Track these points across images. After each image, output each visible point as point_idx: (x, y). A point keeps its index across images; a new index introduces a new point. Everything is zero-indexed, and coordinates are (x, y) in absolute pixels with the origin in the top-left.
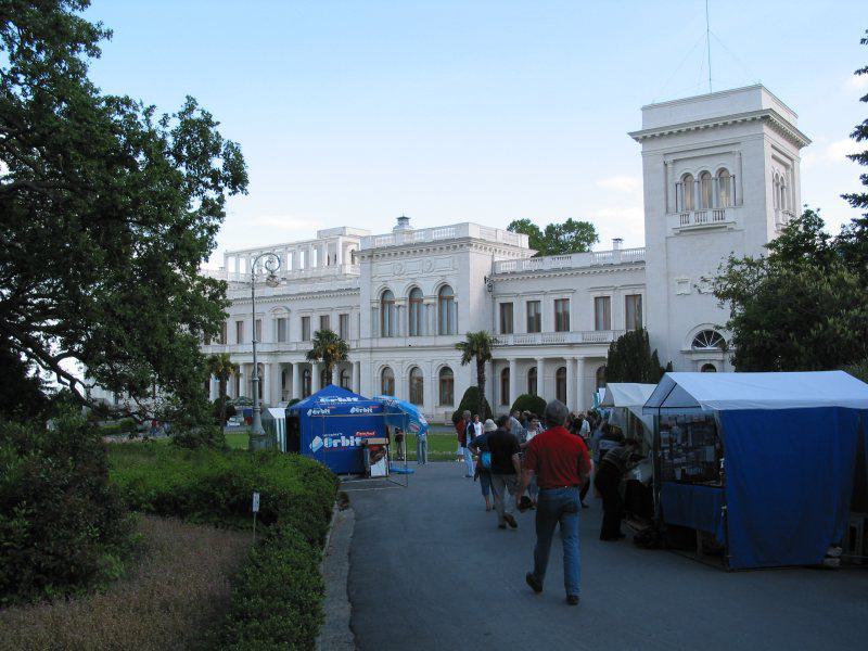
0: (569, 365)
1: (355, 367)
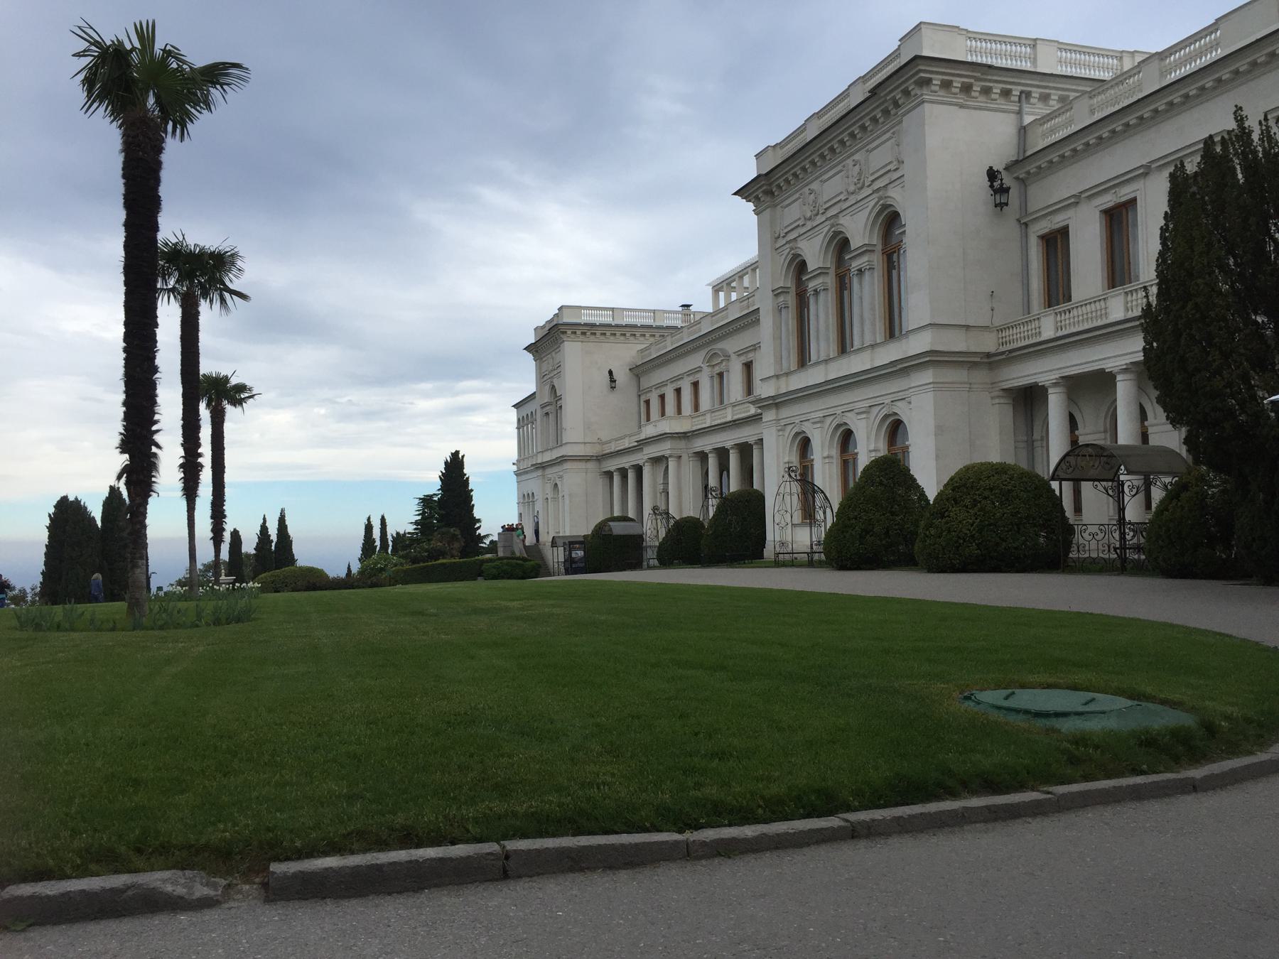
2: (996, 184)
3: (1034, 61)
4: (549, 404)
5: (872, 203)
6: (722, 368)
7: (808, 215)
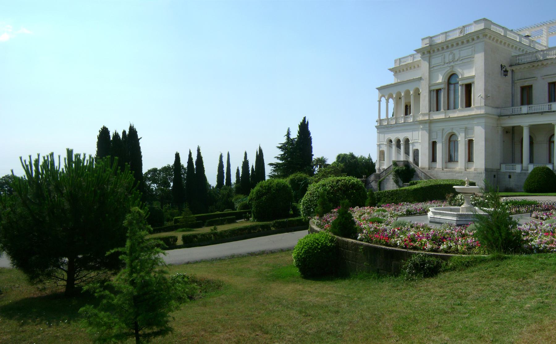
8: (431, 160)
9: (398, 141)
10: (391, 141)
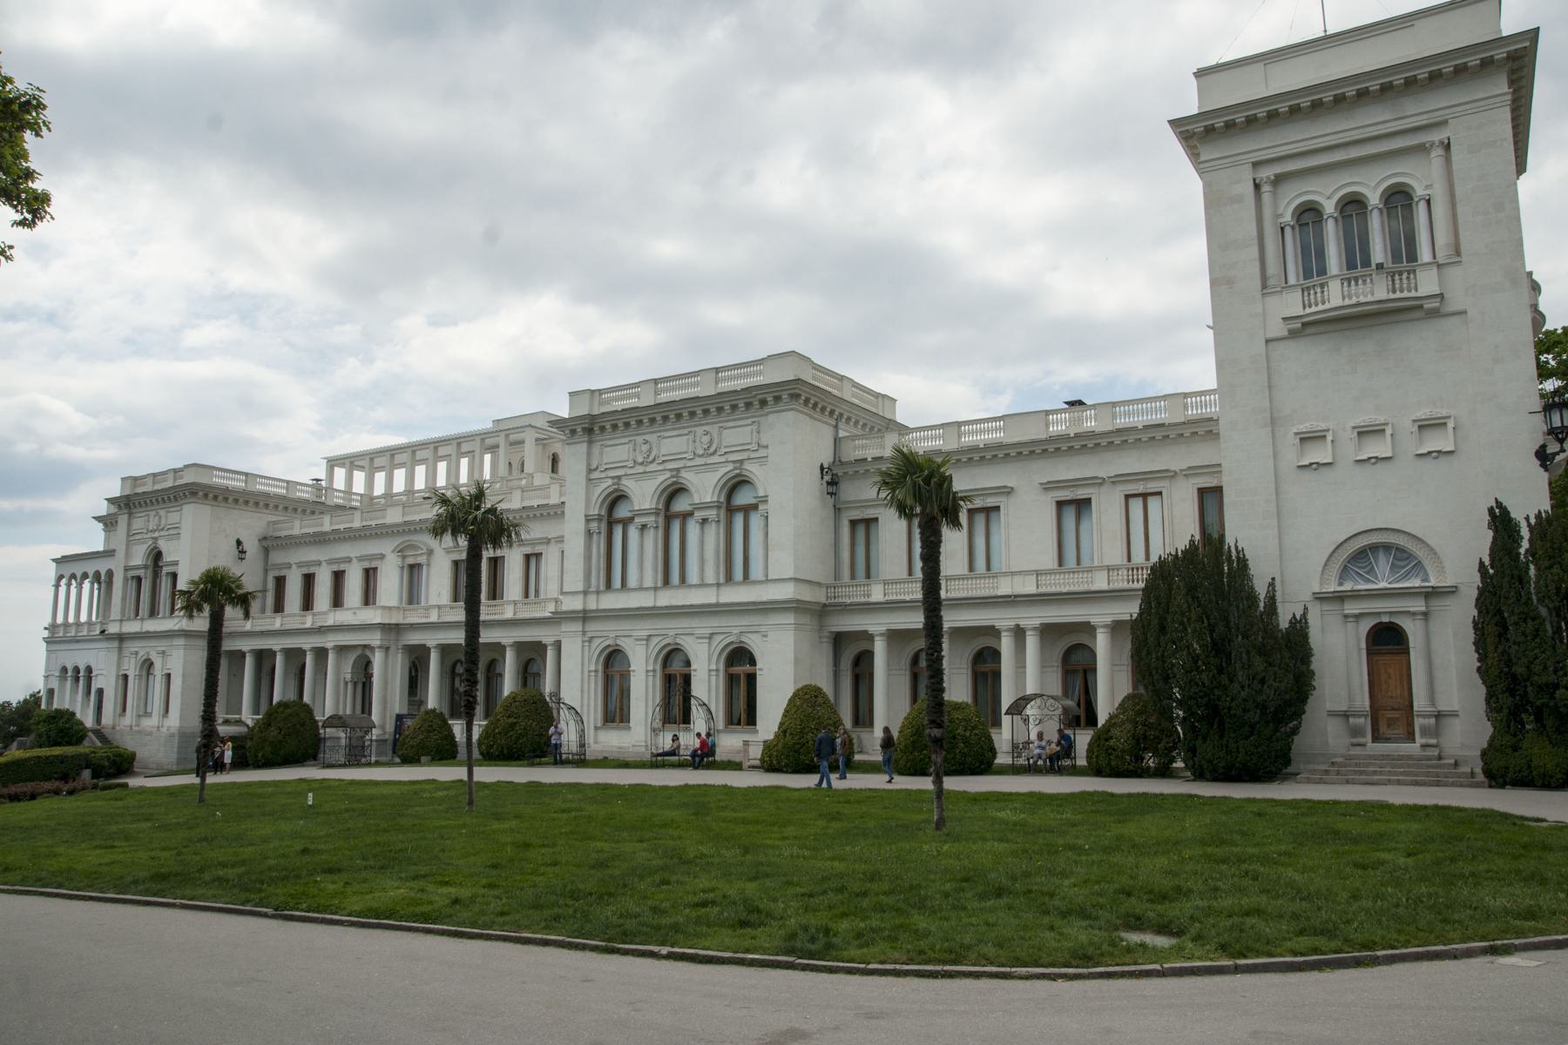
0: (1006, 645)
1: (550, 654)
2: (827, 478)
3: (840, 389)
4: (146, 567)
5: (723, 470)
6: (422, 560)
7: (640, 460)
8: (119, 710)
9: (76, 670)
10: (64, 669)
